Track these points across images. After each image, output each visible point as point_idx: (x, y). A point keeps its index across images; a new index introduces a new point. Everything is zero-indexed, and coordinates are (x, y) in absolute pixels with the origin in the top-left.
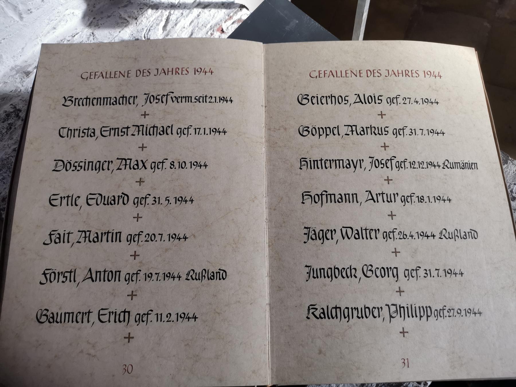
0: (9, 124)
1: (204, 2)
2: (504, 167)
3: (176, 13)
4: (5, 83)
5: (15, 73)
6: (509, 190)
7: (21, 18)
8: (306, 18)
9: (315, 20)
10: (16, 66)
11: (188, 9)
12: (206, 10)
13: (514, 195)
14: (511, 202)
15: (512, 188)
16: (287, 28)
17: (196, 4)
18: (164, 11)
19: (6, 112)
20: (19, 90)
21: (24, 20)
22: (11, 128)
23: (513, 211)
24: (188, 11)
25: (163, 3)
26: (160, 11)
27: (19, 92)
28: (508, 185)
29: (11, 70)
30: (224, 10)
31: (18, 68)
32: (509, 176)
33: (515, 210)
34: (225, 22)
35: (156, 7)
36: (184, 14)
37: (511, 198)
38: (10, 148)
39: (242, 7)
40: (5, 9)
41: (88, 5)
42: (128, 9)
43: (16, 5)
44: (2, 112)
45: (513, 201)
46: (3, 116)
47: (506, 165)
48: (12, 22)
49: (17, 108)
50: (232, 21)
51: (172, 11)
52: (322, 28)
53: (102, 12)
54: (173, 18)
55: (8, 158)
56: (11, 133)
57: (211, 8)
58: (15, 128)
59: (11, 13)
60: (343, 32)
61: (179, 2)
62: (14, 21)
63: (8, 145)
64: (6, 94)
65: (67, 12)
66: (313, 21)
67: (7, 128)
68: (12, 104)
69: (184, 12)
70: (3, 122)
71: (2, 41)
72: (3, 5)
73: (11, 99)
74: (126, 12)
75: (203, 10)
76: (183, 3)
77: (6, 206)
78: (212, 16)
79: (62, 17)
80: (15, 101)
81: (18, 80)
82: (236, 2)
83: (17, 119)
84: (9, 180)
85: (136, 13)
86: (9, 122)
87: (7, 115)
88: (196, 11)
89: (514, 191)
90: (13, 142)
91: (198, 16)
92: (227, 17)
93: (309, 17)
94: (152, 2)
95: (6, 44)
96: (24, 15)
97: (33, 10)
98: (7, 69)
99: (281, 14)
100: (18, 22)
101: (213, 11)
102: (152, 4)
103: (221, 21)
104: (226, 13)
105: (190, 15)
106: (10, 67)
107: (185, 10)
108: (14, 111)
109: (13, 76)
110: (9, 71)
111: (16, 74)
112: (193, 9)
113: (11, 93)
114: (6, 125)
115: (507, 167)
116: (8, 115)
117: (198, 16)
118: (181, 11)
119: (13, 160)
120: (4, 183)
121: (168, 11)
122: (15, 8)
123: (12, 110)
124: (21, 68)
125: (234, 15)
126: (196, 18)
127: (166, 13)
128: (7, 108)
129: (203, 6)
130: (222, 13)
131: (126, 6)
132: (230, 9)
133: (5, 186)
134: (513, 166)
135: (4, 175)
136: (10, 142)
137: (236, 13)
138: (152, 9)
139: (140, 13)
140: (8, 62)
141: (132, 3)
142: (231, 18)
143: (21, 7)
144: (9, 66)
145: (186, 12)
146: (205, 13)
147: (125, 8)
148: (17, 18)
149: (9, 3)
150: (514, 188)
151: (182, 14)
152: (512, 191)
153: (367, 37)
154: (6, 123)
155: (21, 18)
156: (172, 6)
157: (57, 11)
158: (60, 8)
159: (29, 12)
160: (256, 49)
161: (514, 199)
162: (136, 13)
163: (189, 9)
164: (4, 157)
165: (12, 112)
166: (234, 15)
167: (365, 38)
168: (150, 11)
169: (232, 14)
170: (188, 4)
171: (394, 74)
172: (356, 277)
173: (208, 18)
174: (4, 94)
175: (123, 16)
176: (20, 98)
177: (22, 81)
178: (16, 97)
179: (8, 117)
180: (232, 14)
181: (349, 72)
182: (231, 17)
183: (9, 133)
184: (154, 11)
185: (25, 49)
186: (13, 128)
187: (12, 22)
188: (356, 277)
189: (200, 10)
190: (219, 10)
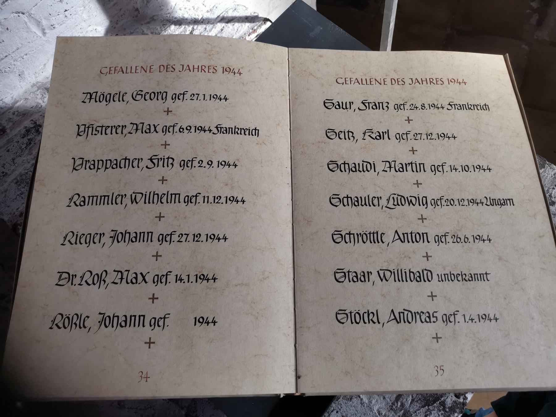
0: (29, 140)
1: (227, 17)
2: (541, 171)
3: (199, 30)
4: (26, 99)
5: (36, 89)
6: (547, 195)
7: (44, 33)
8: (331, 24)
10: (38, 82)
11: (211, 24)
12: (229, 25)
13: (553, 199)
14: (551, 207)
16: (312, 35)
17: (219, 19)
18: (187, 27)
19: (26, 127)
20: (40, 106)
21: (47, 35)
22: (30, 143)
23: (552, 216)
24: (211, 26)
25: (187, 19)
26: (183, 27)
27: (40, 108)
28: (546, 189)
30: (248, 24)
31: (40, 84)
32: (547, 180)
33: (554, 215)
34: (249, 35)
35: (179, 22)
36: (208, 29)
37: (549, 203)
38: (29, 163)
39: (266, 20)
40: (28, 23)
41: (111, 22)
42: (151, 26)
43: (39, 20)
44: (22, 127)
45: (552, 205)
46: (23, 131)
47: (543, 170)
48: (35, 37)
49: (38, 123)
50: (256, 34)
51: (195, 27)
52: (347, 34)
53: (125, 29)
54: (196, 32)
55: (27, 173)
56: (30, 149)
57: (235, 22)
58: (35, 143)
59: (34, 28)
62: (37, 37)
63: (27, 160)
65: (90, 28)
66: (337, 28)
68: (32, 120)
69: (207, 27)
70: (23, 138)
72: (26, 20)
73: (32, 115)
74: (148, 28)
76: (207, 19)
77: (22, 221)
78: (236, 30)
79: (84, 33)
80: (36, 117)
81: (40, 96)
82: (260, 16)
83: (37, 134)
84: (27, 194)
85: (159, 29)
86: (29, 138)
87: (26, 131)
88: (220, 26)
89: (553, 195)
90: (32, 157)
91: (222, 30)
92: (251, 31)
93: (333, 24)
94: (175, 18)
95: (28, 60)
96: (47, 31)
97: (56, 26)
98: (29, 86)
99: (305, 21)
100: (41, 37)
101: (237, 25)
102: (175, 20)
103: (245, 34)
105: (214, 29)
106: (31, 84)
107: (208, 25)
108: (34, 127)
109: (34, 93)
110: (30, 87)
111: (38, 90)
112: (216, 24)
114: (25, 140)
115: (545, 171)
116: (28, 131)
117: (222, 30)
118: (204, 26)
119: (31, 173)
120: (22, 198)
121: (191, 27)
122: (38, 23)
123: (32, 126)
124: (43, 84)
125: (257, 28)
126: (219, 32)
127: (189, 28)
128: (28, 123)
129: (227, 20)
130: (246, 26)
131: (149, 23)
132: (254, 22)
133: (23, 201)
134: (550, 170)
135: (23, 190)
136: (29, 157)
137: (260, 26)
138: (175, 25)
139: (163, 29)
141: (155, 20)
142: (255, 31)
143: (44, 22)
145: (209, 27)
146: (229, 27)
147: (148, 25)
148: (40, 34)
149: (32, 17)
150: (553, 193)
151: (206, 29)
152: (550, 196)
153: (395, 48)
154: (25, 138)
155: (44, 33)
156: (196, 22)
157: (79, 27)
158: (83, 24)
159: (52, 27)
161: (553, 203)
162: (159, 29)
163: (213, 23)
164: (23, 172)
165: (32, 128)
168: (173, 27)
169: (256, 28)
170: (211, 19)
173: (232, 32)
175: (145, 32)
176: (40, 114)
177: (43, 97)
178: (36, 113)
179: (28, 132)
182: (255, 30)
183: (28, 148)
184: (177, 27)
185: (47, 66)
186: (33, 143)
189: (223, 25)
190: (243, 24)
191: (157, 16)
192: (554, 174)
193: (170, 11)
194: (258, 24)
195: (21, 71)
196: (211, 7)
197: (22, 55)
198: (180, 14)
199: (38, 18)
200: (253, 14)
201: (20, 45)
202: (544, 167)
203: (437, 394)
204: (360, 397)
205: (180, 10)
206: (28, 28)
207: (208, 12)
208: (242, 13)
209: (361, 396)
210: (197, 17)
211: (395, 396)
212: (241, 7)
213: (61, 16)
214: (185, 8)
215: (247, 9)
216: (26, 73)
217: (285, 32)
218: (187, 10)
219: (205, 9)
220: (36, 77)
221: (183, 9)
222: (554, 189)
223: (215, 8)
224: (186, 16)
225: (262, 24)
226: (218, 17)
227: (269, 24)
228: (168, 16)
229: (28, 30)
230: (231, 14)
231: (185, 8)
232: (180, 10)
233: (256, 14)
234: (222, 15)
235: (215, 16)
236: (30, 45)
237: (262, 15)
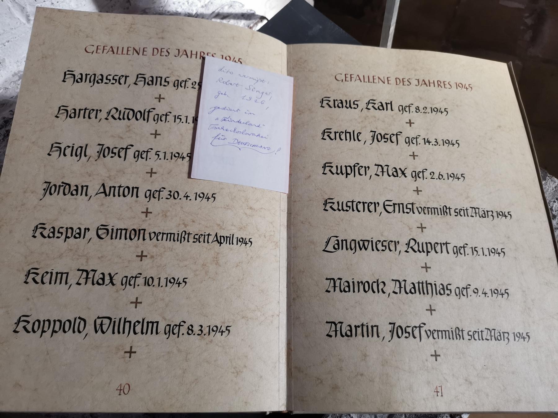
4: (6, 88)
5: (17, 78)
6: (549, 207)
9: (339, 26)
10: (19, 72)
13: (554, 213)
15: (551, 205)
17: (214, 15)
19: (4, 118)
28: (548, 201)
29: (13, 76)
32: (548, 193)
39: (263, 18)
40: (12, 9)
43: (24, 6)
48: (19, 23)
57: (230, 19)
59: (18, 14)
60: (370, 37)
61: (196, 13)
62: (21, 23)
64: (6, 100)
66: (337, 27)
67: (4, 135)
71: (6, 44)
72: (10, 5)
75: (222, 21)
82: (257, 13)
87: (5, 122)
89: (554, 208)
93: (333, 23)
95: (10, 47)
98: (10, 75)
104: (246, 24)
109: (14, 82)
110: (11, 76)
111: (19, 80)
113: (11, 99)
115: (546, 184)
122: (23, 9)
125: (254, 26)
129: (222, 17)
130: (242, 23)
132: (250, 19)
134: (552, 183)
137: (256, 24)
140: (10, 67)
144: (11, 71)
148: (24, 20)
149: (16, 3)
150: (554, 206)
152: (552, 209)
160: (278, 48)
166: (254, 26)
167: (394, 46)
170: (206, 15)
171: (425, 84)
172: (384, 292)
174: (4, 100)
180: (252, 25)
181: (376, 77)
187: (19, 23)
188: (384, 292)
190: (239, 21)
191: (150, 9)
192: (555, 187)
193: (163, 4)
194: (255, 21)
195: (2, 58)
196: (206, 3)
197: (4, 41)
198: (172, 8)
199: (22, 3)
200: (249, 11)
201: (2, 32)
202: (545, 180)
203: (431, 414)
204: (350, 415)
205: (174, 3)
206: (11, 13)
207: (202, 7)
208: (237, 10)
209: (352, 415)
210: (190, 12)
211: (387, 415)
212: (237, 4)
213: (47, 3)
214: (179, 3)
215: (243, 6)
216: (7, 61)
217: (282, 27)
218: (181, 4)
219: (199, 5)
220: (18, 66)
221: (176, 3)
222: (555, 202)
223: (210, 4)
224: (180, 10)
225: (258, 22)
226: (213, 12)
227: (265, 22)
228: (161, 9)
229: (12, 16)
230: (226, 10)
231: (179, 3)
232: (174, 3)
233: (252, 12)
234: (217, 11)
235: (210, 12)
236: (13, 32)
237: (259, 13)
